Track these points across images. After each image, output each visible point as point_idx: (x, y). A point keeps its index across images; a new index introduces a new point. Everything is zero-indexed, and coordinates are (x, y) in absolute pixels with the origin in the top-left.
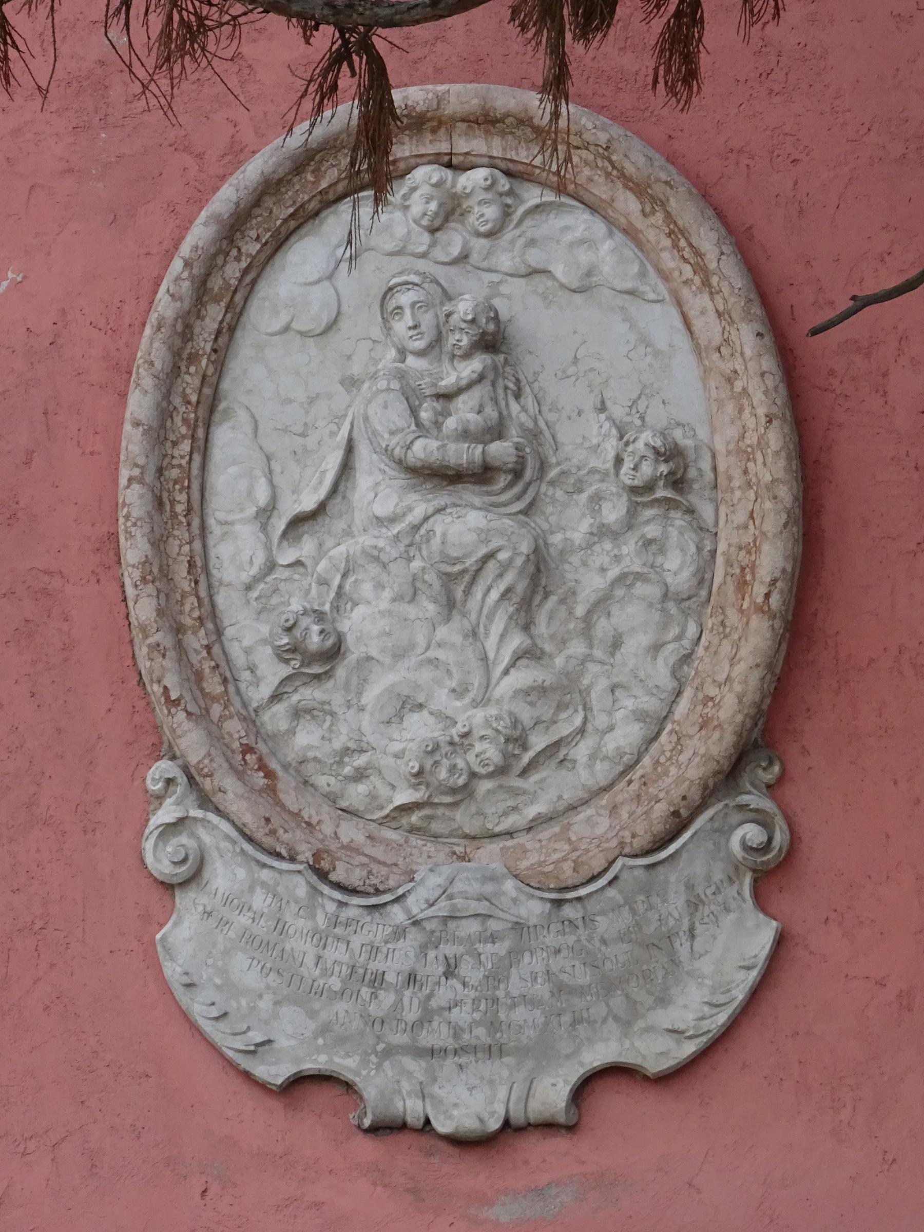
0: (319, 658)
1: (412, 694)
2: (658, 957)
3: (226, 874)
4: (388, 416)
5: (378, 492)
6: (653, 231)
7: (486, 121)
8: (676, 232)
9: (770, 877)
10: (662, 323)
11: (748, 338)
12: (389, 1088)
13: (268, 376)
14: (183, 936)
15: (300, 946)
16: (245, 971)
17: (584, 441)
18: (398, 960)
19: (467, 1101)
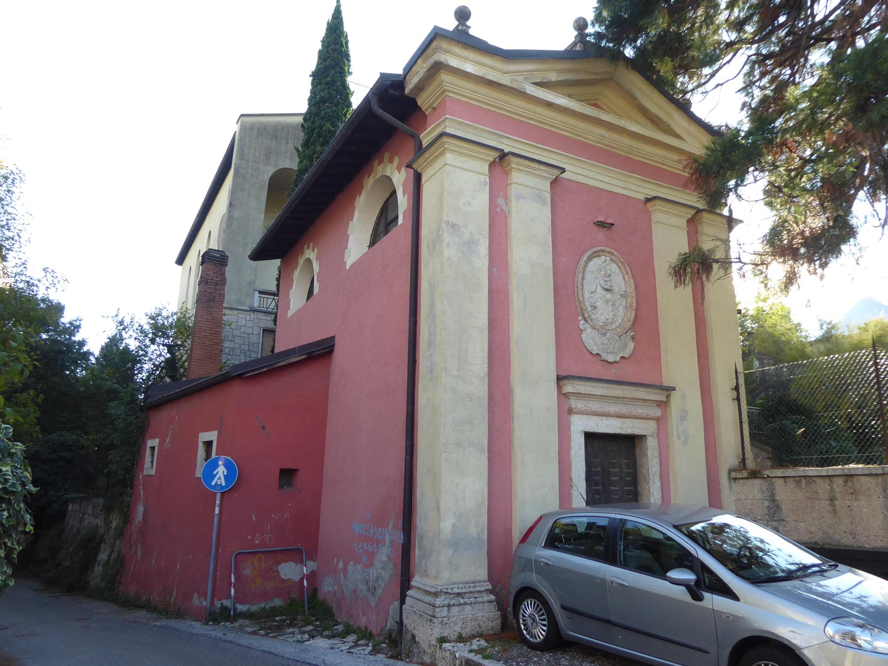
0: (595, 308)
1: (603, 314)
2: (625, 346)
3: (589, 330)
4: (602, 283)
5: (600, 290)
6: (622, 267)
7: (609, 252)
8: (625, 268)
9: (633, 338)
10: (621, 278)
11: (632, 281)
12: (604, 356)
13: (588, 276)
14: (584, 336)
15: (597, 339)
16: (591, 341)
17: (616, 289)
18: (606, 342)
19: (611, 358)
